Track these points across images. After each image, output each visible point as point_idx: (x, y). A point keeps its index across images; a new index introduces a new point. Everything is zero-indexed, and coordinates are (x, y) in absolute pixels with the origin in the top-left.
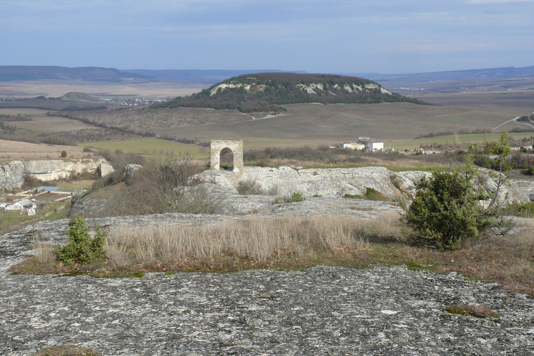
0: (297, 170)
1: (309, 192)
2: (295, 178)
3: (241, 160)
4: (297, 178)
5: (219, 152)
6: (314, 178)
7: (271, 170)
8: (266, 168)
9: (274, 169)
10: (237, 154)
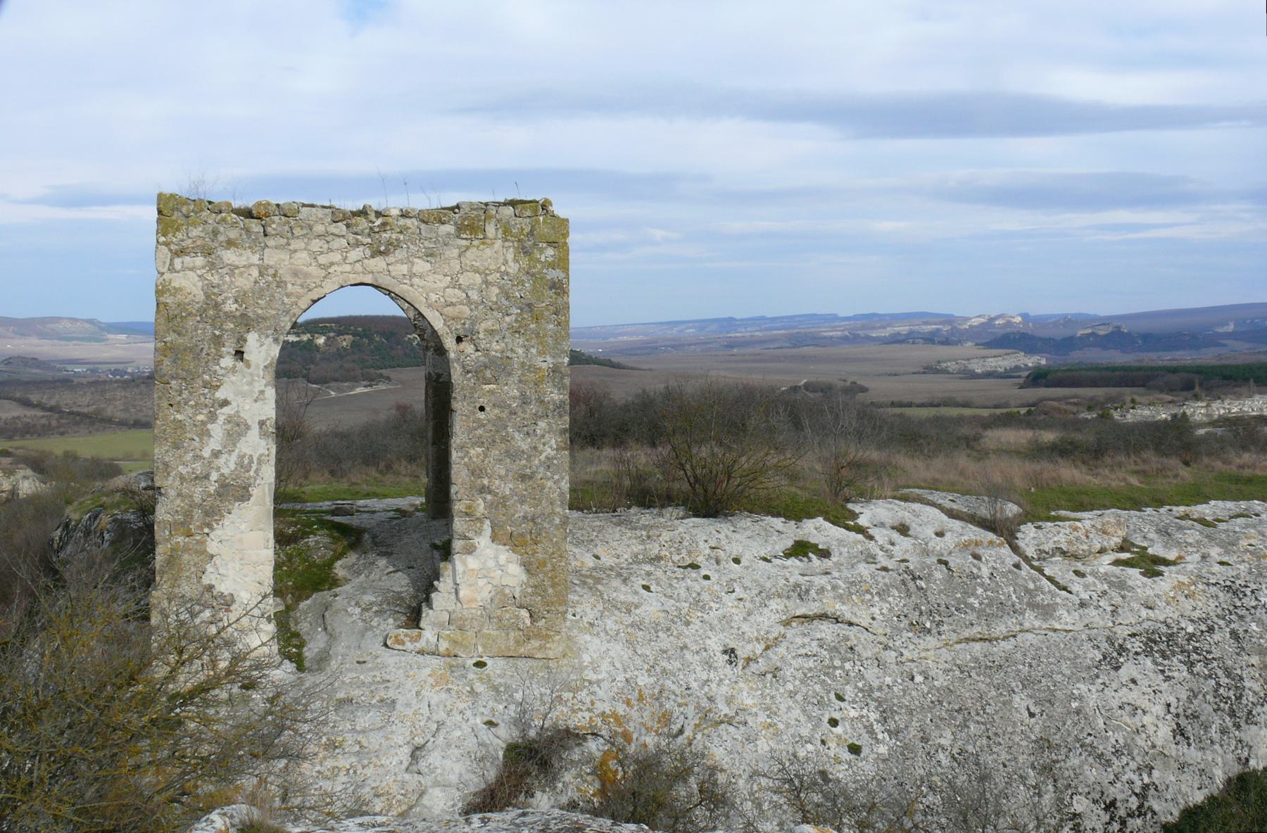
0: (1005, 530)
1: (1193, 754)
2: (1030, 619)
3: (549, 441)
4: (1047, 611)
5: (262, 351)
6: (1164, 599)
7: (801, 549)
8: (745, 522)
9: (818, 530)
10: (498, 368)
